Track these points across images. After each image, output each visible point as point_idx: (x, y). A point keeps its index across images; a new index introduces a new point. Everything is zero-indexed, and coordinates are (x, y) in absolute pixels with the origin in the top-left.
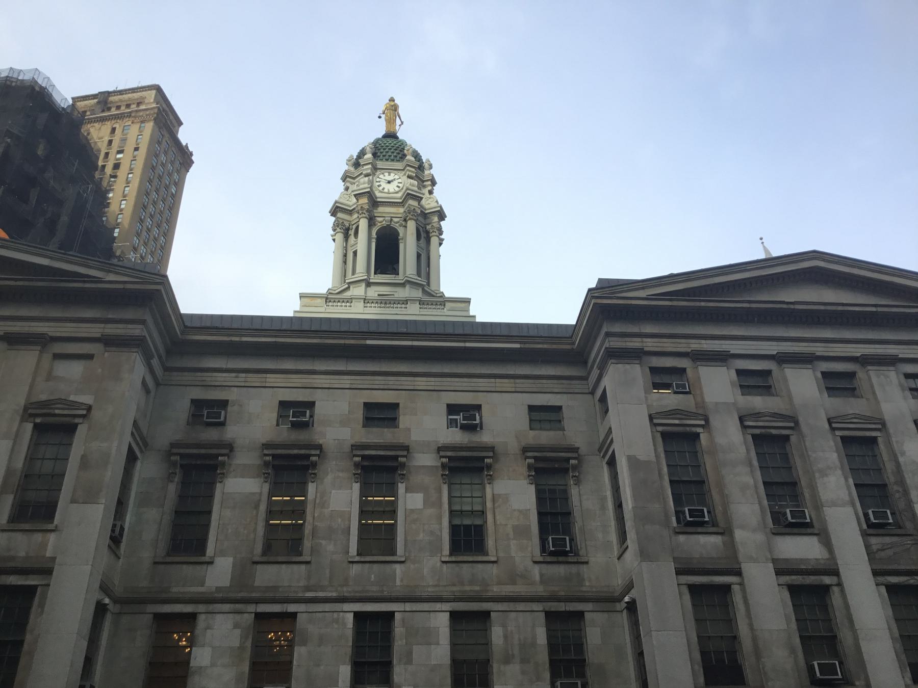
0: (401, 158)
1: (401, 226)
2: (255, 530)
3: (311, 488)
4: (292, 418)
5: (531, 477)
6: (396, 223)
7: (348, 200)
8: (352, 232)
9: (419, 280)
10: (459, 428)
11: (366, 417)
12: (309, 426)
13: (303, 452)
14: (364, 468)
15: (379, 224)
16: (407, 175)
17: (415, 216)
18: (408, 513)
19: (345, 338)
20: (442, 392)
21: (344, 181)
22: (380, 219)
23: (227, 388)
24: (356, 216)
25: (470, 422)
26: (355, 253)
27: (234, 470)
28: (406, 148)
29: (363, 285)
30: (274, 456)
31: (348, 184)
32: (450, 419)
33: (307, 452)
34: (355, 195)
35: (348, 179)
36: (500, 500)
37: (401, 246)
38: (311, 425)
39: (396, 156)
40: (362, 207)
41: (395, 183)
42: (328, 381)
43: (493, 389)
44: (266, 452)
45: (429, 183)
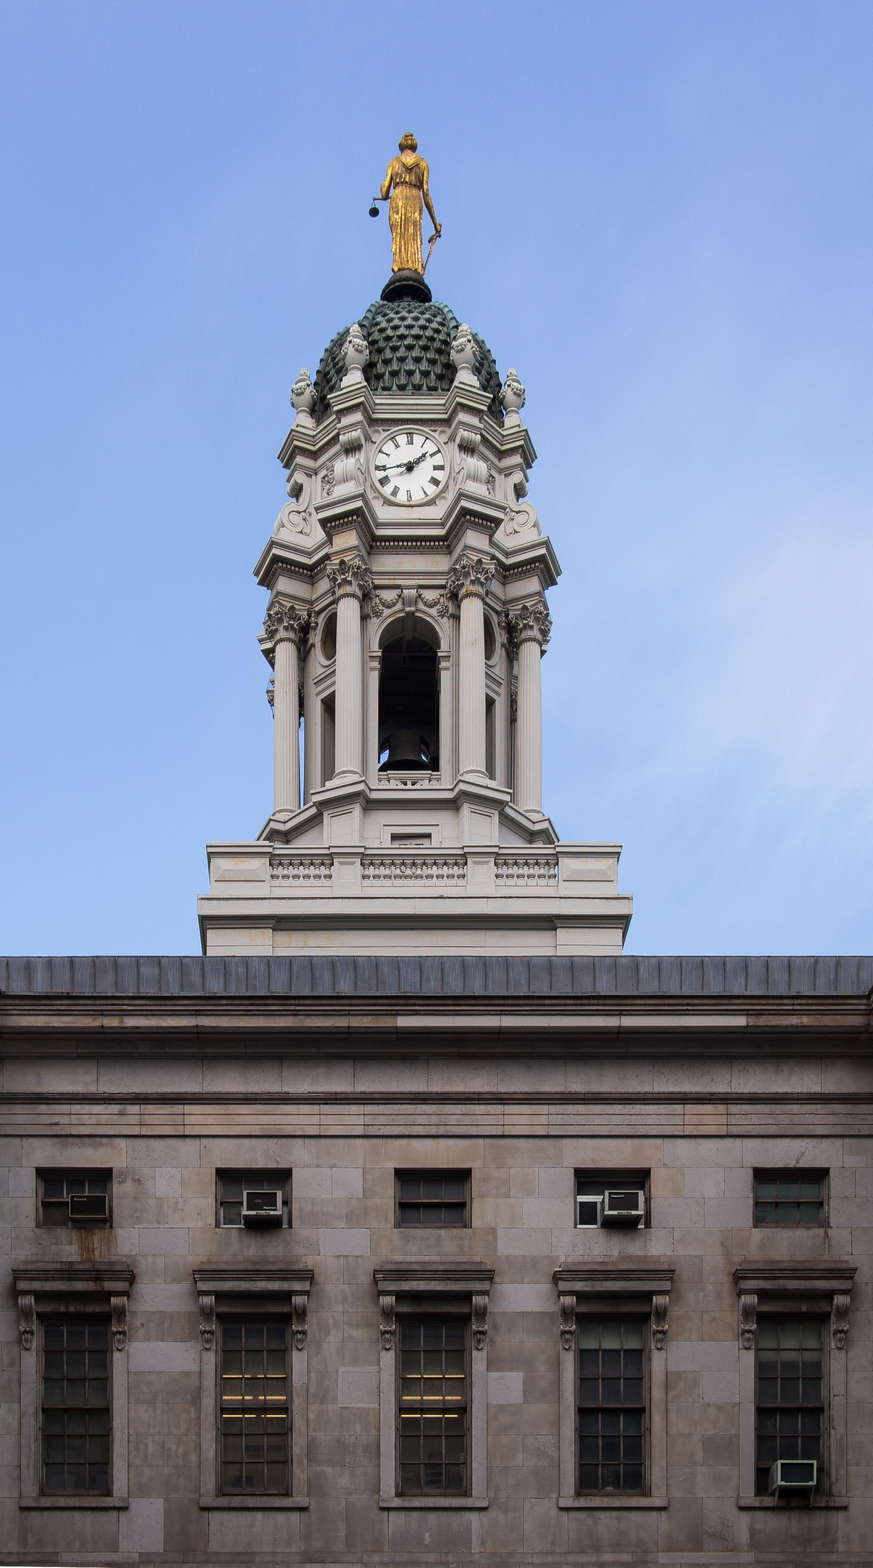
0: (440, 377)
1: (442, 616)
2: (198, 1447)
3: (298, 1360)
4: (248, 1209)
5: (747, 1335)
6: (431, 606)
7: (301, 532)
8: (316, 638)
9: (495, 787)
10: (599, 1223)
11: (400, 1203)
12: (282, 1225)
13: (275, 1286)
14: (401, 1318)
15: (387, 612)
16: (458, 441)
17: (482, 584)
18: (496, 1411)
19: (349, 1014)
20: (565, 1141)
21: (287, 466)
22: (389, 596)
23: (104, 1140)
24: (324, 585)
25: (624, 1212)
26: (329, 705)
27: (142, 1325)
28: (454, 343)
29: (357, 809)
30: (220, 1296)
31: (299, 477)
32: (581, 1203)
33: (286, 1286)
34: (324, 522)
35: (299, 460)
36: (681, 1384)
37: (445, 679)
38: (285, 1226)
39: (425, 374)
40: (342, 562)
41: (425, 471)
42: (316, 1120)
43: (678, 1131)
44: (202, 1286)
45: (517, 459)
